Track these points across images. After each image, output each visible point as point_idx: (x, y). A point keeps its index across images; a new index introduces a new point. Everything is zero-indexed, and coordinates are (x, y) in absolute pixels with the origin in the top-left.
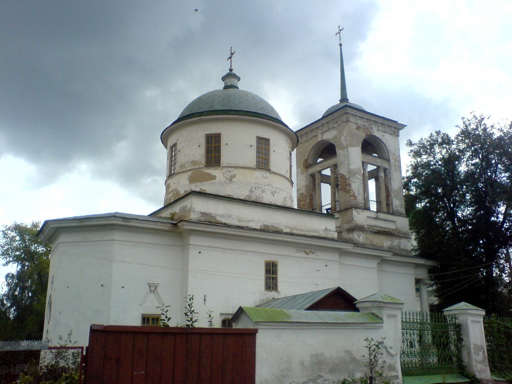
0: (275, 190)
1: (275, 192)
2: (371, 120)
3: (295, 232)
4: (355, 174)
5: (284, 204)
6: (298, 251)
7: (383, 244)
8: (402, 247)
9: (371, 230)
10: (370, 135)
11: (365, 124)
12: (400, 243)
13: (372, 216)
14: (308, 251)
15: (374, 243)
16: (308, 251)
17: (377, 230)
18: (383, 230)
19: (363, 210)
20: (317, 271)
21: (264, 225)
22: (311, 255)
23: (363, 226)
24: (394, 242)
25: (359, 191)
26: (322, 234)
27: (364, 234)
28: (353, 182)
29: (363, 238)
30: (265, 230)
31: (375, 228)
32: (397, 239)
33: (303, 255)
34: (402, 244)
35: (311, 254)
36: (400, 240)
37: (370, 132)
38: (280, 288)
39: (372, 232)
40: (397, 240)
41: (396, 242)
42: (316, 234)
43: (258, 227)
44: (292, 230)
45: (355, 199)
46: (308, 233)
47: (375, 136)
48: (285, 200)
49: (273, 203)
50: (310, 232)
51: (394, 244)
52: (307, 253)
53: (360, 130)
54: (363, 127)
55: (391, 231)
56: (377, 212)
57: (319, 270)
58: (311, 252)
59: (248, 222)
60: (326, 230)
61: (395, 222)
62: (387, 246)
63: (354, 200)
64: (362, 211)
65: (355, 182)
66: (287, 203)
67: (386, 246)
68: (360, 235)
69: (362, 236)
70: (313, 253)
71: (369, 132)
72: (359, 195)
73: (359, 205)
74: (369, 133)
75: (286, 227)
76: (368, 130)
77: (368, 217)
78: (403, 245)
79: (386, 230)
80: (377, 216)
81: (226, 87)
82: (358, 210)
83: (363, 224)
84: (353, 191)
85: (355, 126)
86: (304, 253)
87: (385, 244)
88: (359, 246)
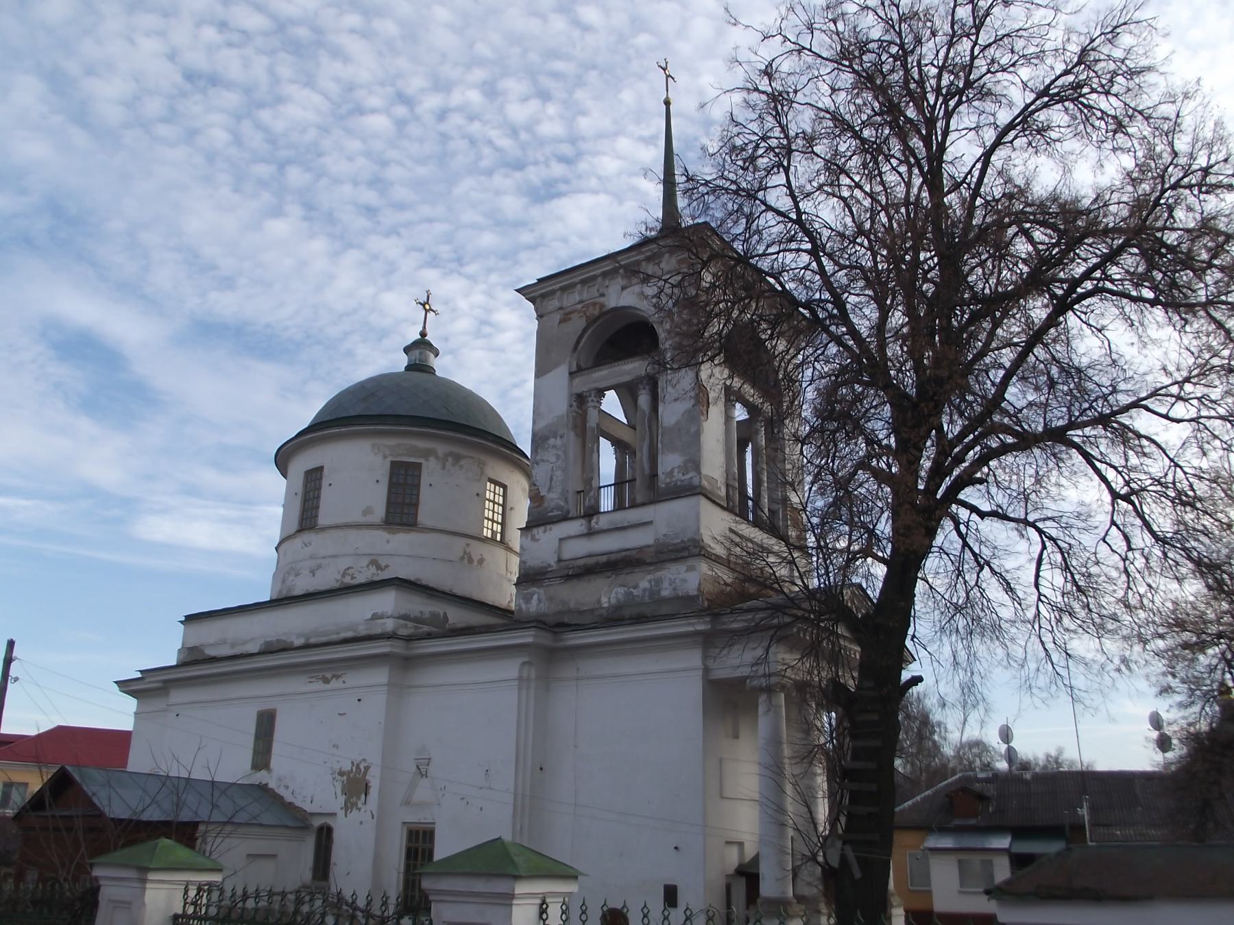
0: (319, 561)
1: (319, 567)
2: (594, 278)
3: (313, 641)
4: (547, 438)
5: (342, 582)
6: (314, 680)
7: (599, 601)
8: (665, 593)
9: (565, 572)
10: (602, 314)
11: (585, 296)
12: (659, 582)
13: (572, 533)
14: (329, 675)
15: (572, 605)
16: (329, 675)
17: (585, 566)
18: (604, 559)
19: (548, 527)
20: (341, 715)
21: (267, 643)
22: (334, 684)
23: (545, 567)
24: (636, 587)
25: (551, 479)
26: (363, 631)
27: (542, 591)
28: (537, 464)
29: (539, 600)
30: (270, 650)
31: (581, 562)
32: (649, 572)
33: (320, 686)
34: (666, 584)
35: (334, 679)
36: (659, 574)
37: (602, 306)
38: (273, 764)
39: (568, 575)
40: (649, 577)
41: (643, 582)
42: (350, 634)
43: (257, 651)
44: (308, 639)
45: (540, 505)
46: (334, 637)
47: (616, 310)
48: (344, 575)
49: (311, 589)
50: (339, 633)
51: (635, 592)
52: (326, 681)
53: (570, 319)
54: (579, 306)
55: (634, 553)
56: (615, 510)
57: (344, 714)
58: (334, 676)
59: (245, 643)
60: (375, 617)
61: (651, 523)
62: (609, 602)
63: (536, 507)
64: (545, 531)
65: (543, 461)
66: (353, 578)
67: (606, 605)
68: (532, 595)
69: (535, 597)
70: (337, 677)
71: (598, 307)
72: (549, 490)
73: (550, 514)
74: (596, 312)
75: (299, 636)
76: (594, 304)
77: (561, 540)
78: (671, 585)
79: (613, 557)
80: (590, 528)
81: (409, 368)
82: (535, 531)
83: (544, 565)
84: (535, 485)
85: (557, 317)
86: (321, 682)
87: (604, 600)
88: (534, 624)
